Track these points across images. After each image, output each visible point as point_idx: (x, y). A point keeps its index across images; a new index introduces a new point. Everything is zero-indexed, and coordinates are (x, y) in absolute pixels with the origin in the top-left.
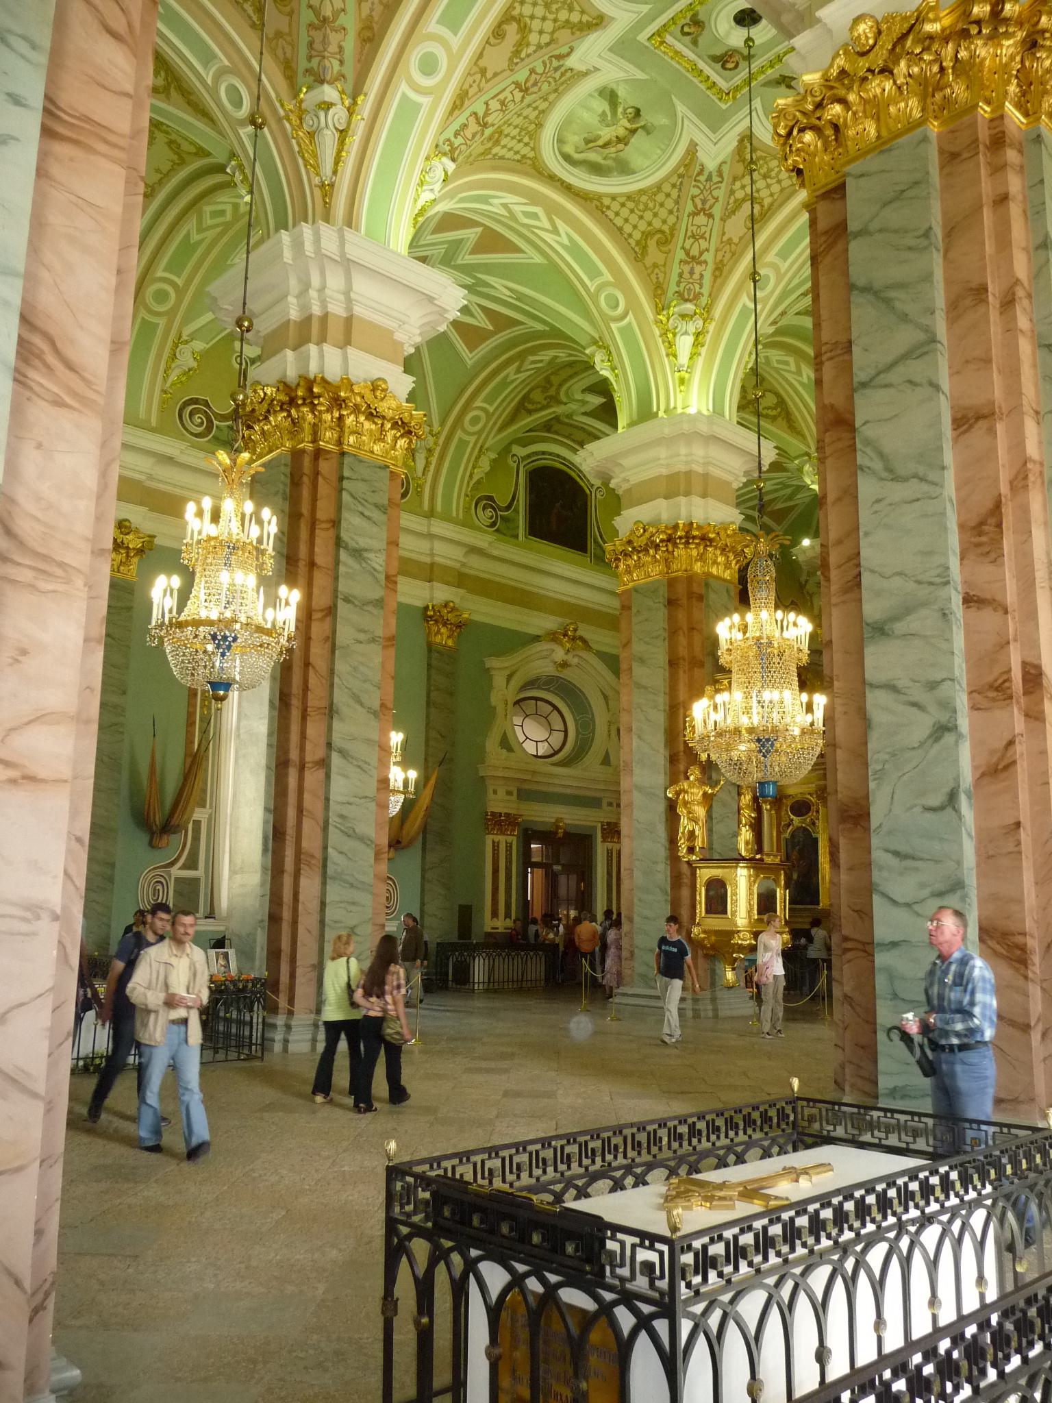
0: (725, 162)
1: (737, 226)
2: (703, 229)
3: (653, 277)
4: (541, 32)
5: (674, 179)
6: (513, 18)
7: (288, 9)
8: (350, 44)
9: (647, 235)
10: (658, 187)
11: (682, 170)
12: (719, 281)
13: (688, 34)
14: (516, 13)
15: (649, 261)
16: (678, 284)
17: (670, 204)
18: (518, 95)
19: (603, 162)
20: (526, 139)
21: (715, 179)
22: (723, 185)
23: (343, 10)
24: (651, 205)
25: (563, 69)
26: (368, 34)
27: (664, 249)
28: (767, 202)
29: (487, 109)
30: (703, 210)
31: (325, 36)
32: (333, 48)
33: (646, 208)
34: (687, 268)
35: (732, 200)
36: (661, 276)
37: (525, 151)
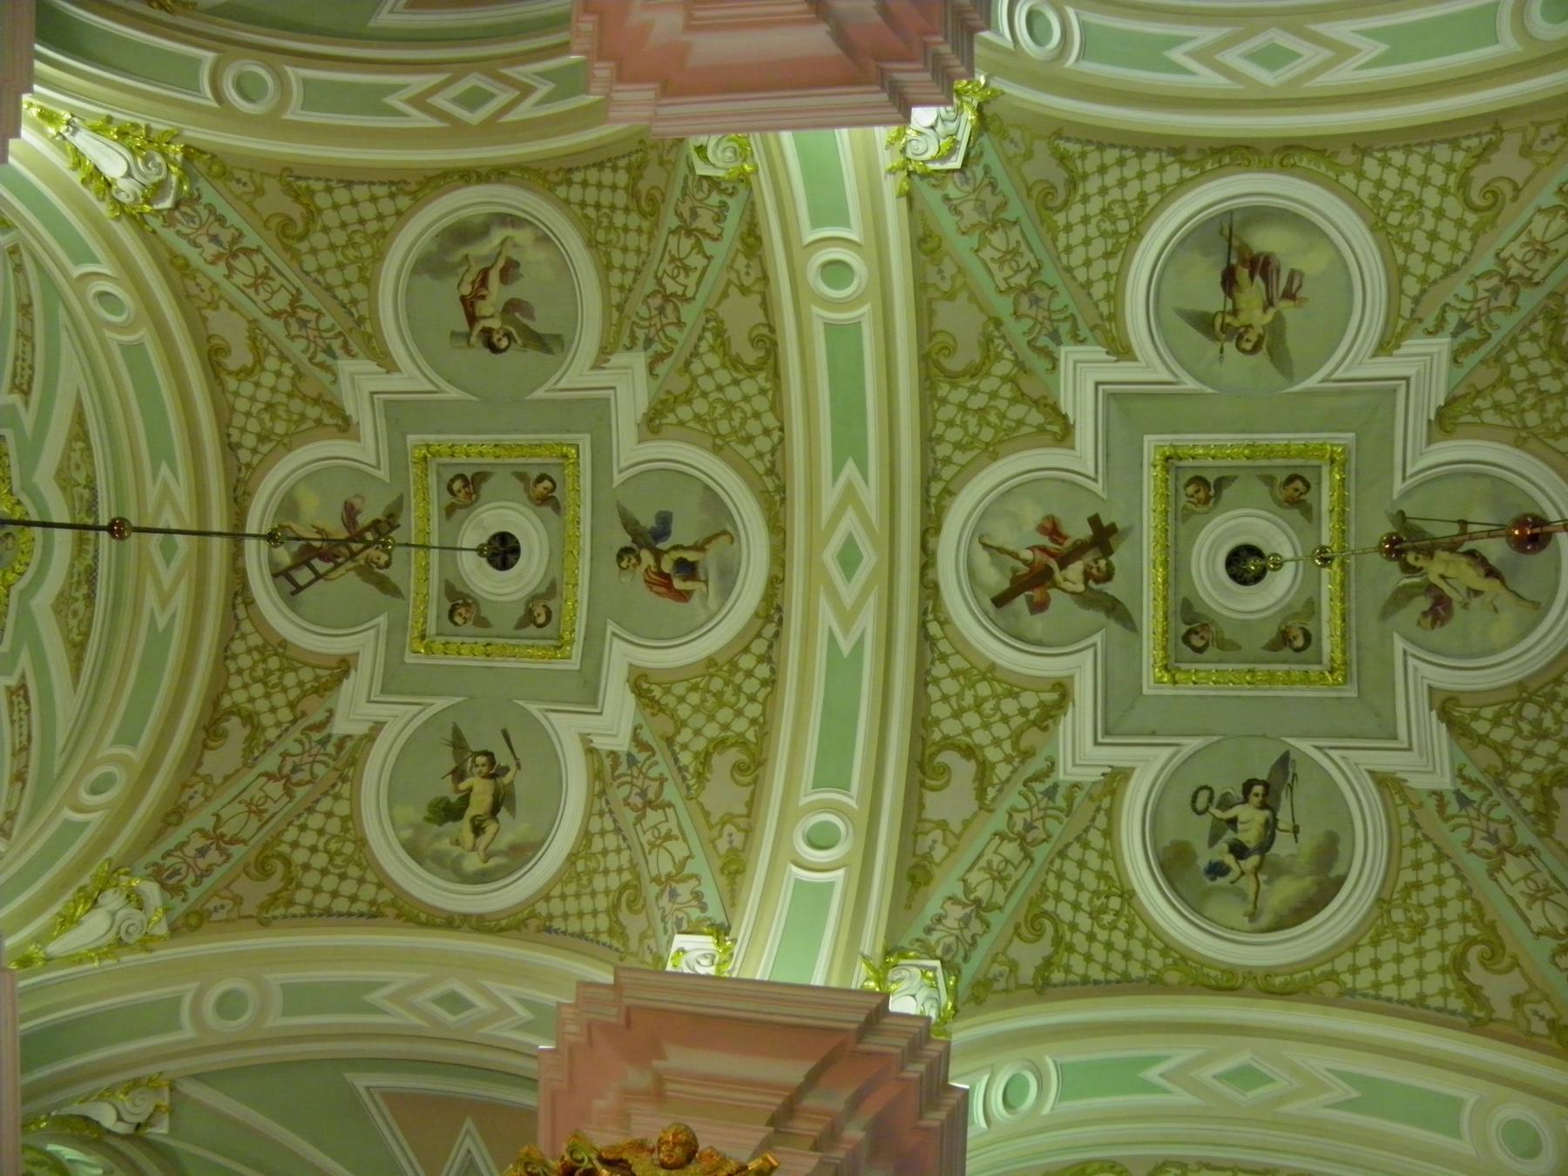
0: (335, 381)
1: (229, 329)
2: (264, 295)
3: (245, 177)
4: (709, 372)
5: (363, 309)
6: (759, 368)
7: (1035, 193)
8: (946, 222)
9: (312, 214)
10: (369, 282)
11: (368, 327)
12: (167, 256)
13: (541, 479)
14: (761, 377)
15: (272, 186)
16: (211, 209)
17: (334, 278)
18: (671, 287)
19: (464, 251)
20: (591, 212)
21: (321, 357)
22: (305, 358)
23: (977, 251)
24: (351, 253)
25: (640, 343)
26: (930, 245)
27: (274, 223)
28: (232, 383)
29: (701, 251)
30: (293, 314)
31: (986, 213)
32: (968, 208)
33: (351, 243)
34: (226, 236)
35: (272, 349)
36: (238, 189)
37: (576, 193)
